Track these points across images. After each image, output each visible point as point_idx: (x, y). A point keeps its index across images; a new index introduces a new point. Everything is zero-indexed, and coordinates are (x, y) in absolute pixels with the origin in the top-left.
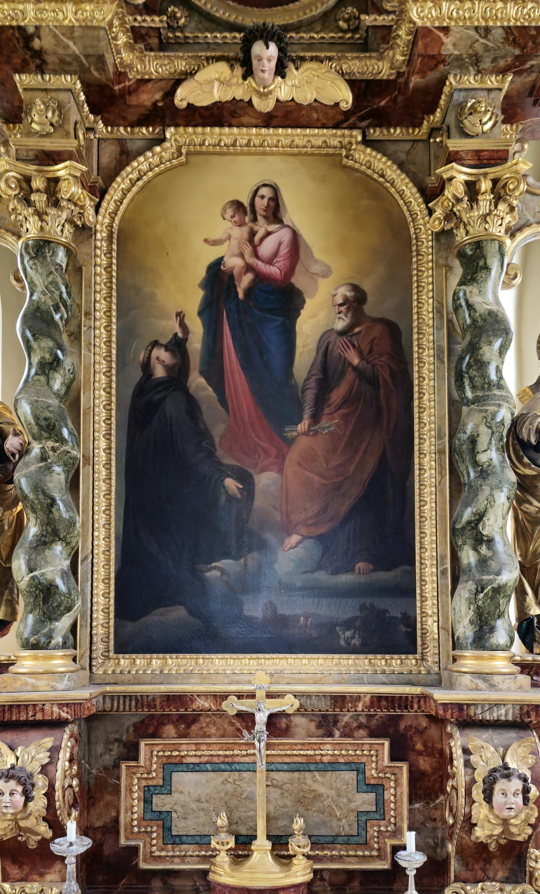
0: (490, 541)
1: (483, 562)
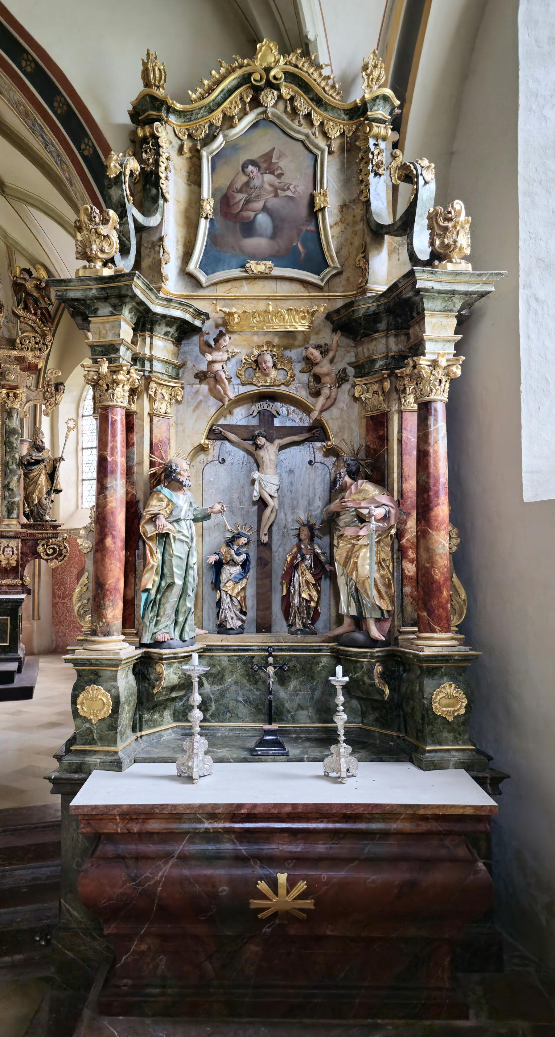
0: (12, 490)
1: (10, 495)
